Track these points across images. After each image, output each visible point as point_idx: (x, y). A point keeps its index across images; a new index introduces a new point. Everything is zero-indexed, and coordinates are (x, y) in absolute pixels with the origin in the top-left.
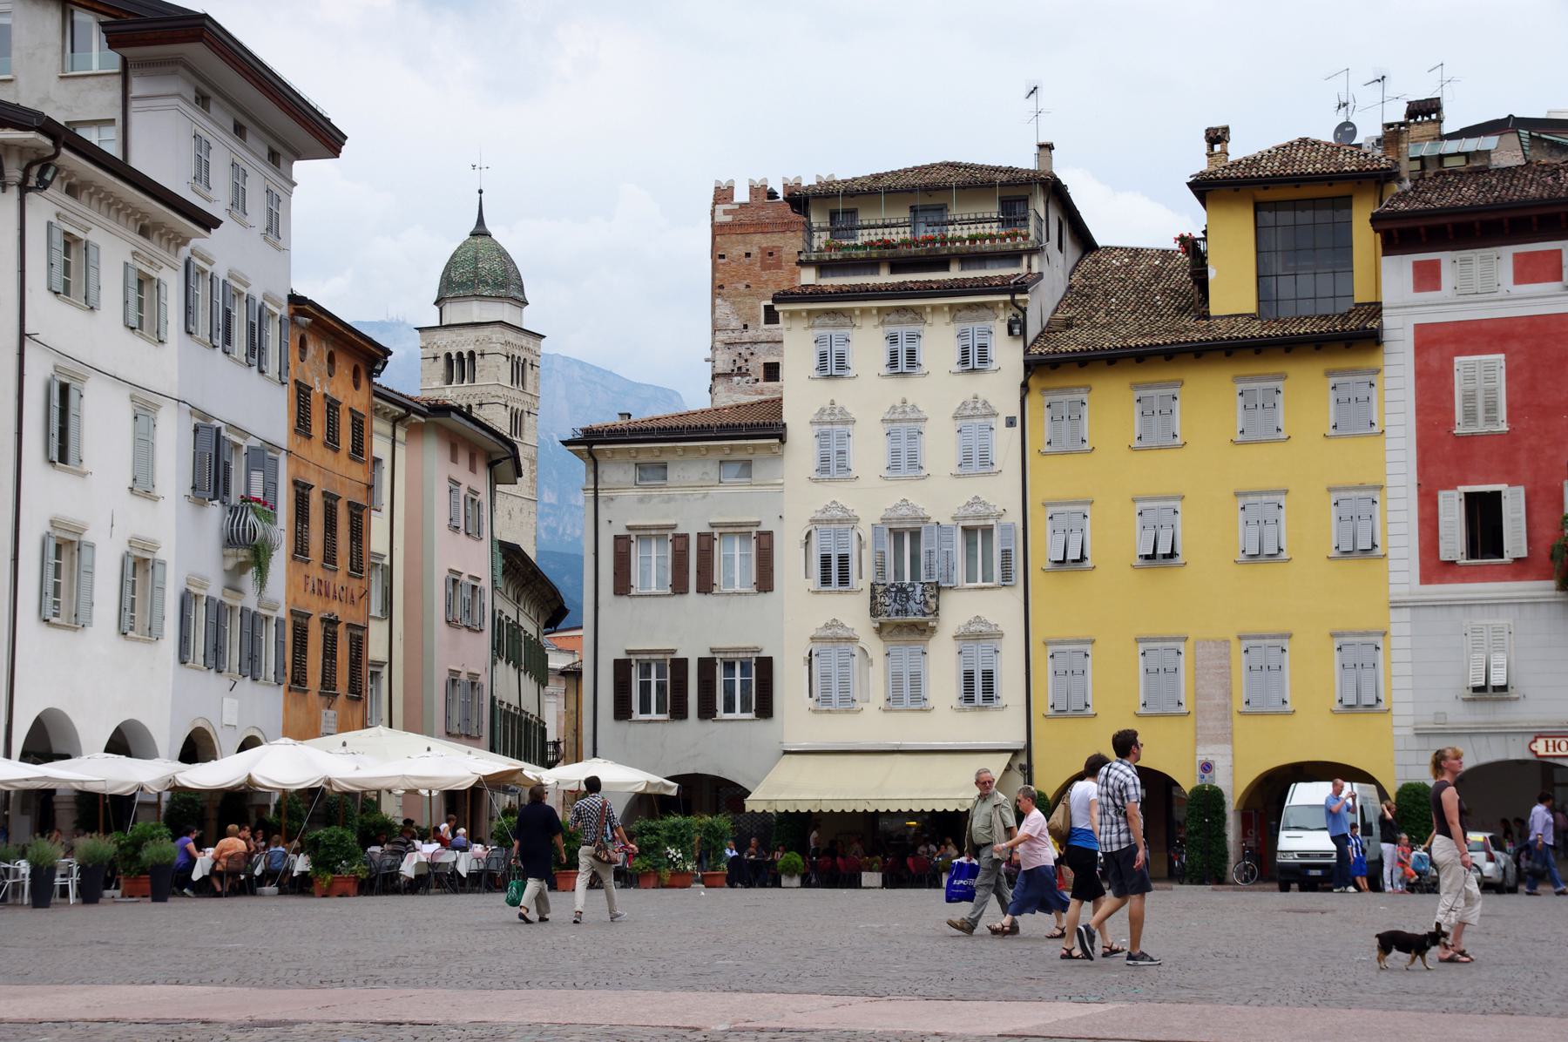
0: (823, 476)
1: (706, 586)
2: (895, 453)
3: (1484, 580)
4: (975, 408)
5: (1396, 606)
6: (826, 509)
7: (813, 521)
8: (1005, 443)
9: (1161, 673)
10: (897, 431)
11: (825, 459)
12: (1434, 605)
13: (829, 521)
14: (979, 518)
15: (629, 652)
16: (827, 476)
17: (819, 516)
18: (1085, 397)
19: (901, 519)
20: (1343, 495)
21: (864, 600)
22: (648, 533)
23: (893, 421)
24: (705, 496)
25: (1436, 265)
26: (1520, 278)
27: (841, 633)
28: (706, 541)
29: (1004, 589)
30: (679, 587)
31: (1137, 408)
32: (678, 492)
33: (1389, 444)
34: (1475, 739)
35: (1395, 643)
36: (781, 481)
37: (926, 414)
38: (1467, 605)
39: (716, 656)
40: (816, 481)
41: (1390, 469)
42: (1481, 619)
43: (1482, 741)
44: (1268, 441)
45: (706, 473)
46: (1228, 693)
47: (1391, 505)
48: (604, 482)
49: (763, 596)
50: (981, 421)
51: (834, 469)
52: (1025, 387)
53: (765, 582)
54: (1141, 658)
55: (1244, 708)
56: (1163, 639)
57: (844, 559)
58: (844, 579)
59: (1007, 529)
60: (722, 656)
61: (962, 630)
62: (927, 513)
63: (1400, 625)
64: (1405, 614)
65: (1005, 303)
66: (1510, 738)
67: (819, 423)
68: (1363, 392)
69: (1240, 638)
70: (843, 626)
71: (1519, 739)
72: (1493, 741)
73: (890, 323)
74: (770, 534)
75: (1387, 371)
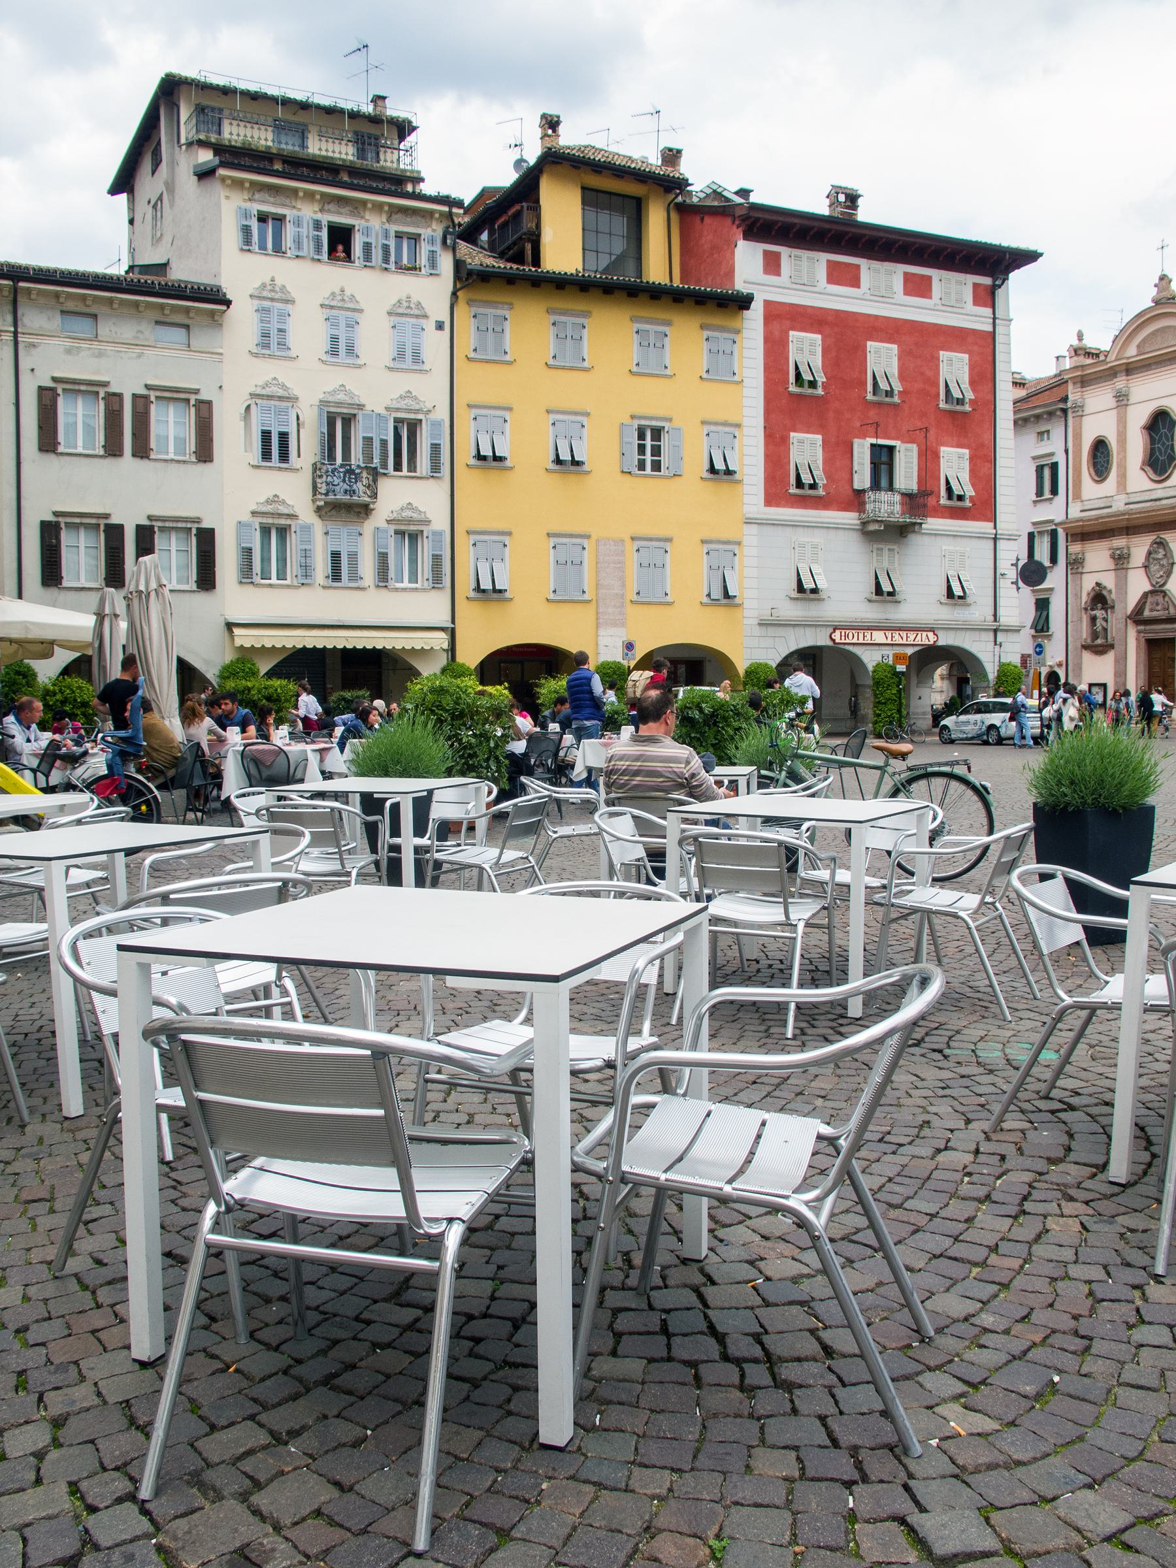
0: (264, 351)
1: (142, 450)
2: (334, 339)
3: (805, 507)
4: (409, 307)
5: (749, 522)
6: (267, 385)
7: (253, 395)
8: (435, 345)
9: (568, 565)
10: (336, 318)
11: (266, 335)
12: (774, 524)
13: (270, 397)
14: (409, 411)
15: (56, 514)
16: (267, 352)
17: (259, 391)
18: (507, 314)
19: (339, 404)
20: (713, 428)
21: (306, 477)
22: (77, 387)
23: (332, 307)
24: (140, 356)
25: (777, 256)
26: (831, 279)
27: (283, 510)
28: (142, 404)
29: (431, 480)
30: (113, 449)
31: (552, 331)
32: (109, 348)
33: (746, 392)
34: (796, 629)
35: (746, 551)
36: (221, 351)
37: (362, 306)
38: (794, 525)
39: (154, 523)
40: (256, 355)
41: (746, 412)
42: (803, 536)
43: (801, 631)
44: (657, 376)
45: (141, 332)
46: (623, 585)
47: (746, 441)
48: (24, 326)
49: (202, 467)
50: (414, 321)
51: (274, 346)
52: (454, 294)
53: (204, 452)
54: (552, 551)
55: (635, 598)
56: (571, 536)
57: (284, 437)
58: (284, 456)
59: (437, 424)
60: (160, 524)
61: (395, 515)
62: (363, 401)
63: (750, 535)
64: (754, 529)
65: (441, 213)
66: (818, 629)
67: (259, 298)
68: (727, 347)
69: (633, 539)
70: (284, 502)
71: (823, 629)
72: (809, 631)
73: (329, 211)
74: (209, 403)
75: (745, 333)
